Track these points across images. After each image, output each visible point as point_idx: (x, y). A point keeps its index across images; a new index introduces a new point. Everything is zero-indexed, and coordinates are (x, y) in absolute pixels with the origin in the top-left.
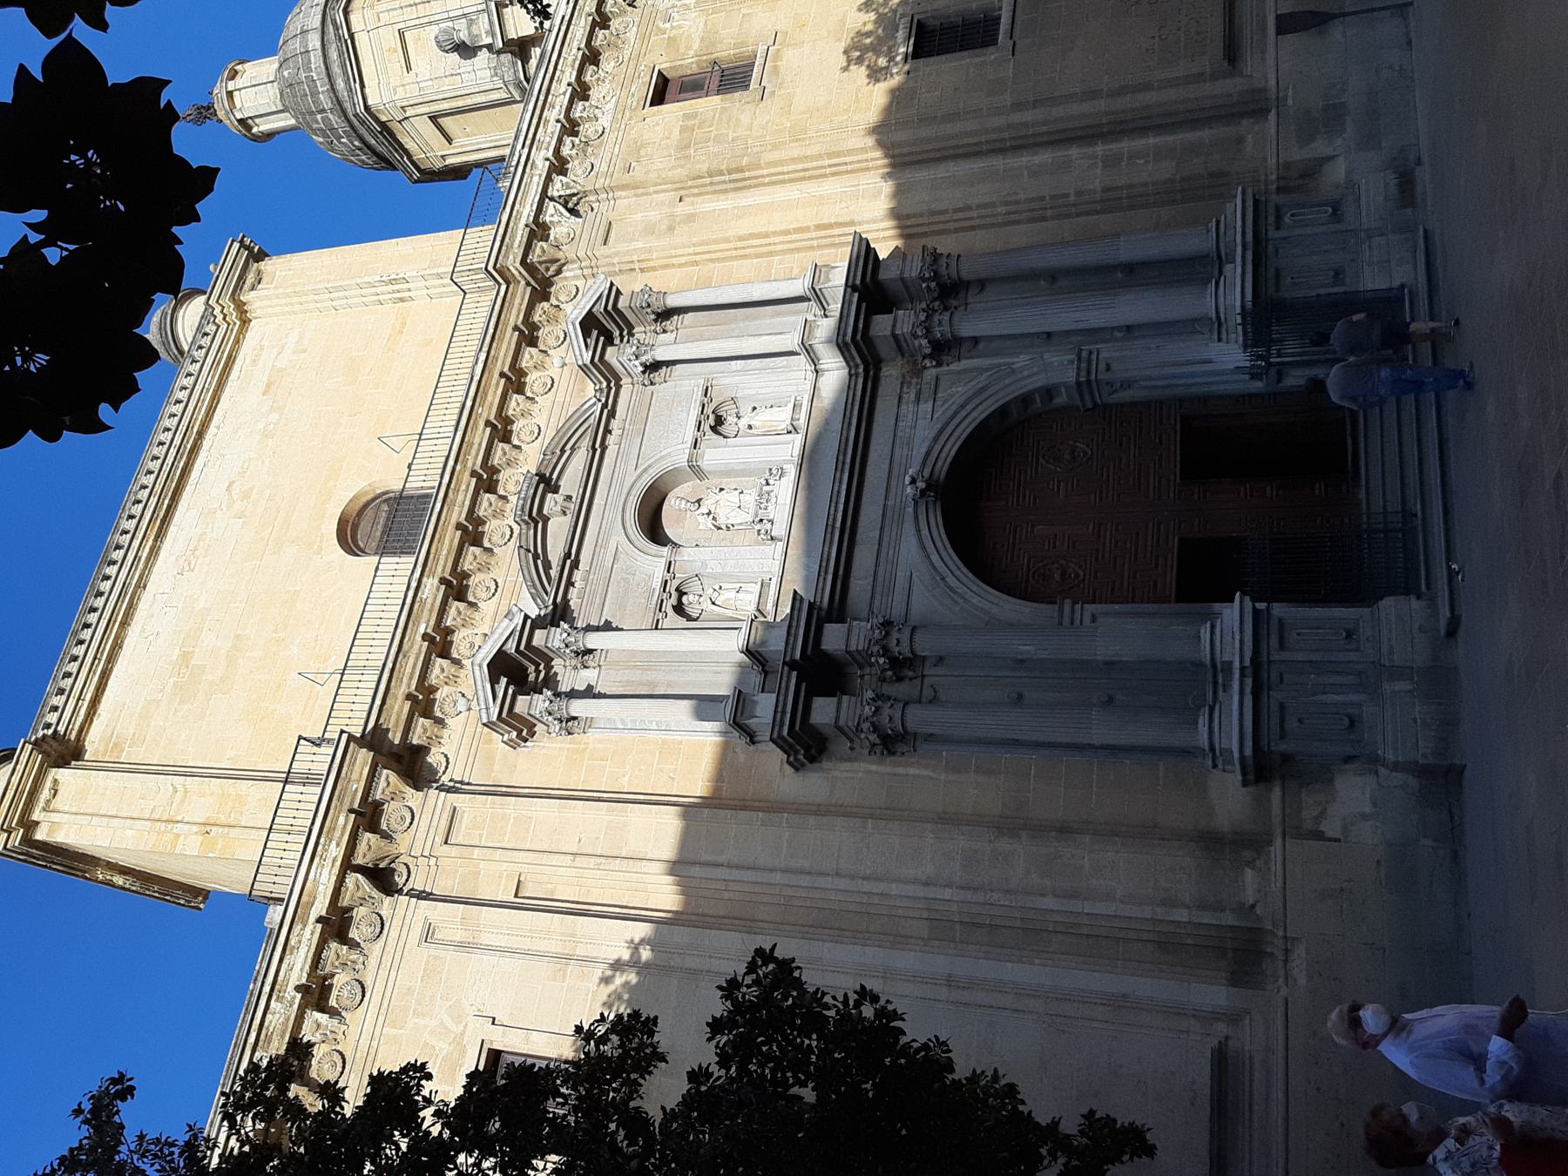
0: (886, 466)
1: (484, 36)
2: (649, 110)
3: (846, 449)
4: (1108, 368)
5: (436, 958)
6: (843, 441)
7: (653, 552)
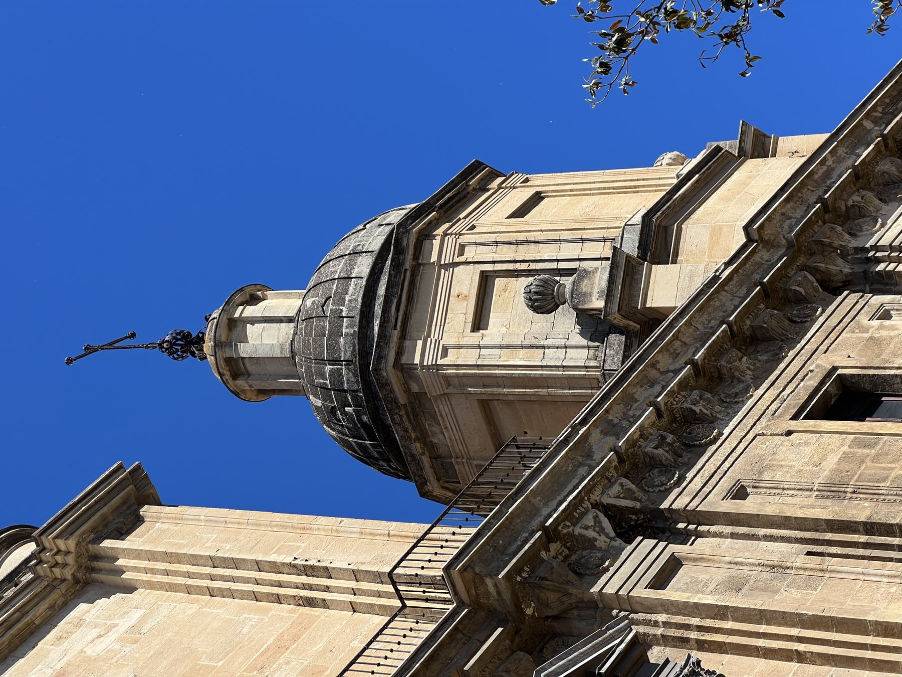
1: (595, 296)
2: (801, 424)
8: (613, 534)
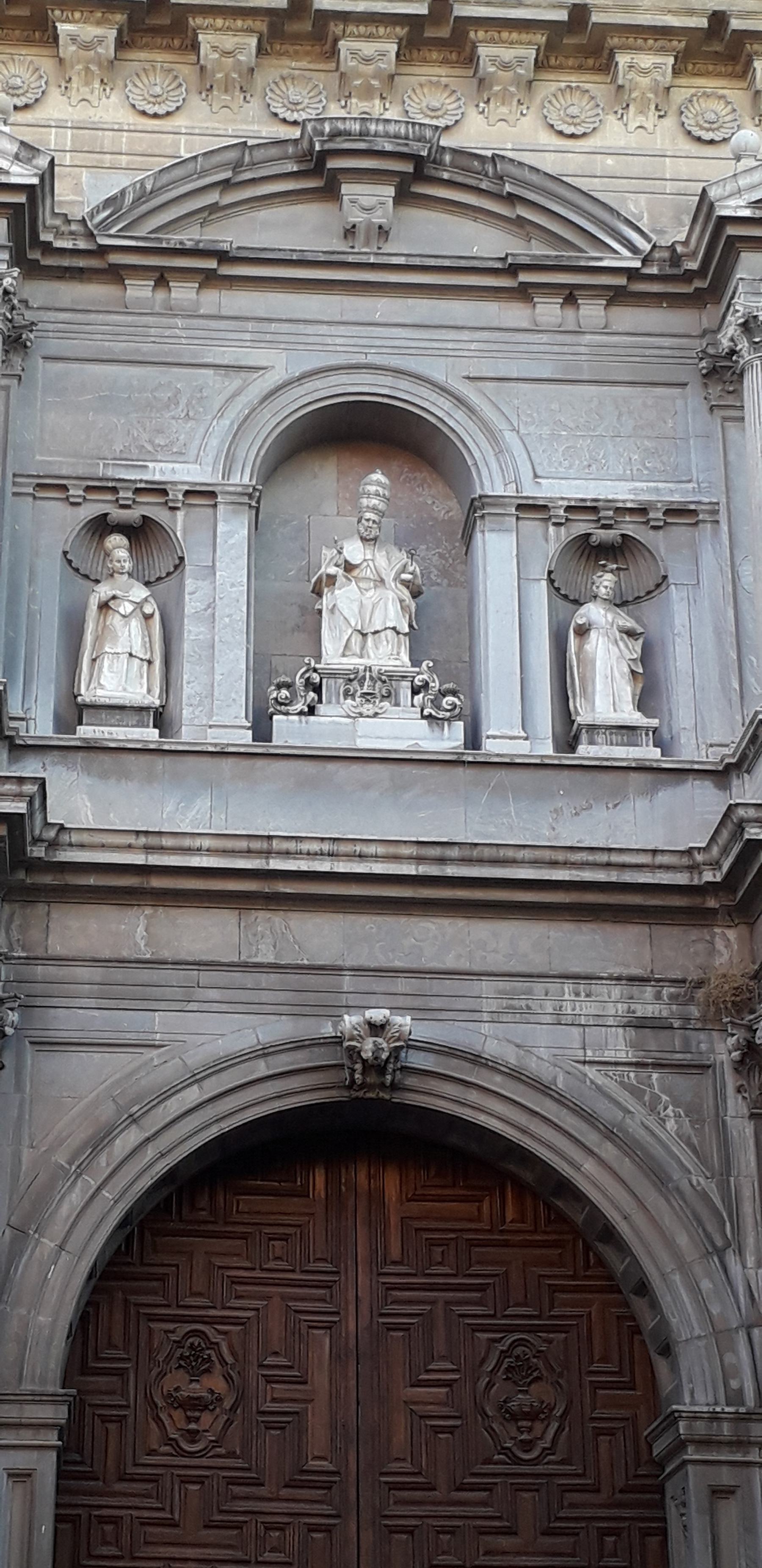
0: (450, 962)
3: (481, 861)
6: (502, 853)
7: (241, 454)
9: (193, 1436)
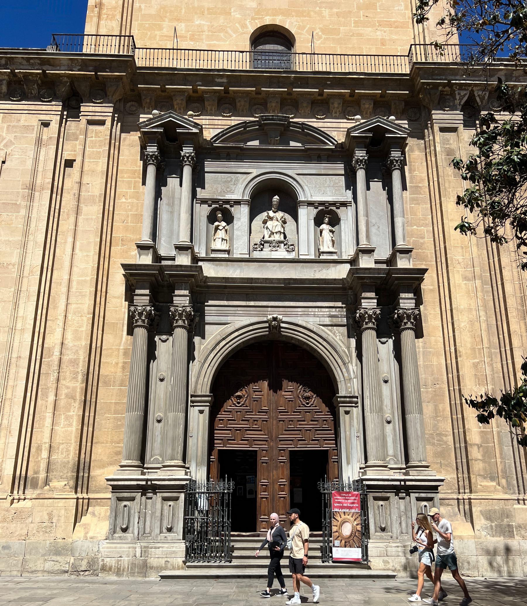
4: (347, 413)
5: (33, 129)
8: (462, 103)
9: (239, 403)
